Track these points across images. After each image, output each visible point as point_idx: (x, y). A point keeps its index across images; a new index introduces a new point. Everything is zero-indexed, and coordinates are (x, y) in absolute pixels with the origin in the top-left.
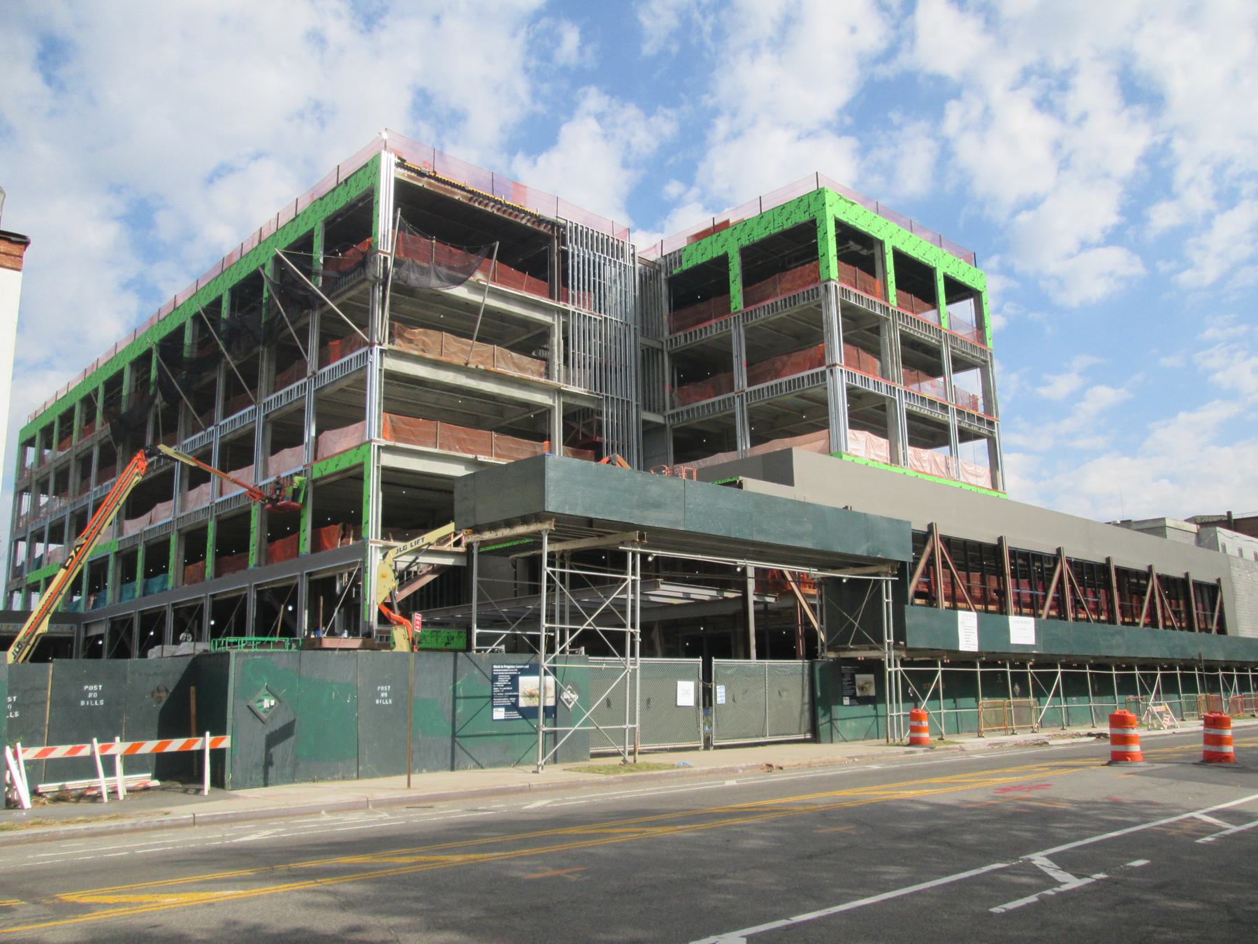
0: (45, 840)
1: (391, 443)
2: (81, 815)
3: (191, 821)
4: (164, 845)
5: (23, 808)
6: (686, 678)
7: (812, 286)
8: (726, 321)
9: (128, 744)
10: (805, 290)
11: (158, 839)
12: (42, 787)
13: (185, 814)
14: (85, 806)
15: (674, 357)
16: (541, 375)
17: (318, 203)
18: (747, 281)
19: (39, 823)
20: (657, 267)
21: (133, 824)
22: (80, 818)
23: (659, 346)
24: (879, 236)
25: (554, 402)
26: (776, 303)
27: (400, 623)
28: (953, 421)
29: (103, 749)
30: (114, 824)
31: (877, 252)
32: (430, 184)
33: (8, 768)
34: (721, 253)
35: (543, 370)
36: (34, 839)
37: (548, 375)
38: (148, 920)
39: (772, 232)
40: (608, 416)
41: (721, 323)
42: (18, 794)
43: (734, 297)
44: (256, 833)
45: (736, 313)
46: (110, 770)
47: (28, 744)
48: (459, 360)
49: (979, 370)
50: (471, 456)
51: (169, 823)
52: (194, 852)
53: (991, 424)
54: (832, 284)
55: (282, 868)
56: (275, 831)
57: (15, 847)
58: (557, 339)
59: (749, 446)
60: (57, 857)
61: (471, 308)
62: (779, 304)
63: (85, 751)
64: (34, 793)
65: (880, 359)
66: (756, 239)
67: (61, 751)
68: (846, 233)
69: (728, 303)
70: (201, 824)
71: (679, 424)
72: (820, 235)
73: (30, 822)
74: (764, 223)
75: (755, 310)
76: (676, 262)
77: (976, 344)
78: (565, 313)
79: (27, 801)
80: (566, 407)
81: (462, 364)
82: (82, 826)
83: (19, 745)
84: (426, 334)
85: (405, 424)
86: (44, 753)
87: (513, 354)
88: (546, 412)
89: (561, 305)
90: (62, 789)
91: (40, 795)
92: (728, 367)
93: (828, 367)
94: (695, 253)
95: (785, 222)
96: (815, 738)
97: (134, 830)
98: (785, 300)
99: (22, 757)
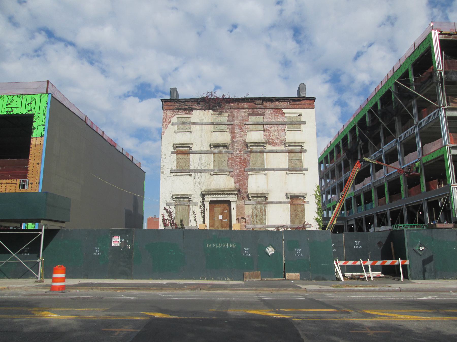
0: (351, 292)
2: (360, 284)
3: (399, 290)
4: (391, 297)
5: (341, 280)
9: (372, 262)
11: (389, 295)
12: (346, 274)
13: (396, 287)
14: (360, 281)
17: (408, 59)
19: (348, 286)
21: (379, 289)
22: (360, 285)
29: (364, 263)
30: (372, 288)
32: (455, 37)
33: (335, 267)
36: (348, 291)
38: (396, 323)
42: (339, 275)
44: (426, 297)
46: (367, 271)
47: (339, 260)
51: (392, 290)
52: (404, 301)
55: (442, 311)
56: (433, 296)
57: (343, 293)
60: (357, 298)
63: (358, 263)
64: (344, 276)
67: (350, 263)
70: (403, 291)
73: (345, 285)
79: (342, 279)
82: (362, 288)
83: (337, 260)
86: (345, 263)
90: (352, 275)
91: (346, 277)
97: (379, 291)
99: (339, 264)
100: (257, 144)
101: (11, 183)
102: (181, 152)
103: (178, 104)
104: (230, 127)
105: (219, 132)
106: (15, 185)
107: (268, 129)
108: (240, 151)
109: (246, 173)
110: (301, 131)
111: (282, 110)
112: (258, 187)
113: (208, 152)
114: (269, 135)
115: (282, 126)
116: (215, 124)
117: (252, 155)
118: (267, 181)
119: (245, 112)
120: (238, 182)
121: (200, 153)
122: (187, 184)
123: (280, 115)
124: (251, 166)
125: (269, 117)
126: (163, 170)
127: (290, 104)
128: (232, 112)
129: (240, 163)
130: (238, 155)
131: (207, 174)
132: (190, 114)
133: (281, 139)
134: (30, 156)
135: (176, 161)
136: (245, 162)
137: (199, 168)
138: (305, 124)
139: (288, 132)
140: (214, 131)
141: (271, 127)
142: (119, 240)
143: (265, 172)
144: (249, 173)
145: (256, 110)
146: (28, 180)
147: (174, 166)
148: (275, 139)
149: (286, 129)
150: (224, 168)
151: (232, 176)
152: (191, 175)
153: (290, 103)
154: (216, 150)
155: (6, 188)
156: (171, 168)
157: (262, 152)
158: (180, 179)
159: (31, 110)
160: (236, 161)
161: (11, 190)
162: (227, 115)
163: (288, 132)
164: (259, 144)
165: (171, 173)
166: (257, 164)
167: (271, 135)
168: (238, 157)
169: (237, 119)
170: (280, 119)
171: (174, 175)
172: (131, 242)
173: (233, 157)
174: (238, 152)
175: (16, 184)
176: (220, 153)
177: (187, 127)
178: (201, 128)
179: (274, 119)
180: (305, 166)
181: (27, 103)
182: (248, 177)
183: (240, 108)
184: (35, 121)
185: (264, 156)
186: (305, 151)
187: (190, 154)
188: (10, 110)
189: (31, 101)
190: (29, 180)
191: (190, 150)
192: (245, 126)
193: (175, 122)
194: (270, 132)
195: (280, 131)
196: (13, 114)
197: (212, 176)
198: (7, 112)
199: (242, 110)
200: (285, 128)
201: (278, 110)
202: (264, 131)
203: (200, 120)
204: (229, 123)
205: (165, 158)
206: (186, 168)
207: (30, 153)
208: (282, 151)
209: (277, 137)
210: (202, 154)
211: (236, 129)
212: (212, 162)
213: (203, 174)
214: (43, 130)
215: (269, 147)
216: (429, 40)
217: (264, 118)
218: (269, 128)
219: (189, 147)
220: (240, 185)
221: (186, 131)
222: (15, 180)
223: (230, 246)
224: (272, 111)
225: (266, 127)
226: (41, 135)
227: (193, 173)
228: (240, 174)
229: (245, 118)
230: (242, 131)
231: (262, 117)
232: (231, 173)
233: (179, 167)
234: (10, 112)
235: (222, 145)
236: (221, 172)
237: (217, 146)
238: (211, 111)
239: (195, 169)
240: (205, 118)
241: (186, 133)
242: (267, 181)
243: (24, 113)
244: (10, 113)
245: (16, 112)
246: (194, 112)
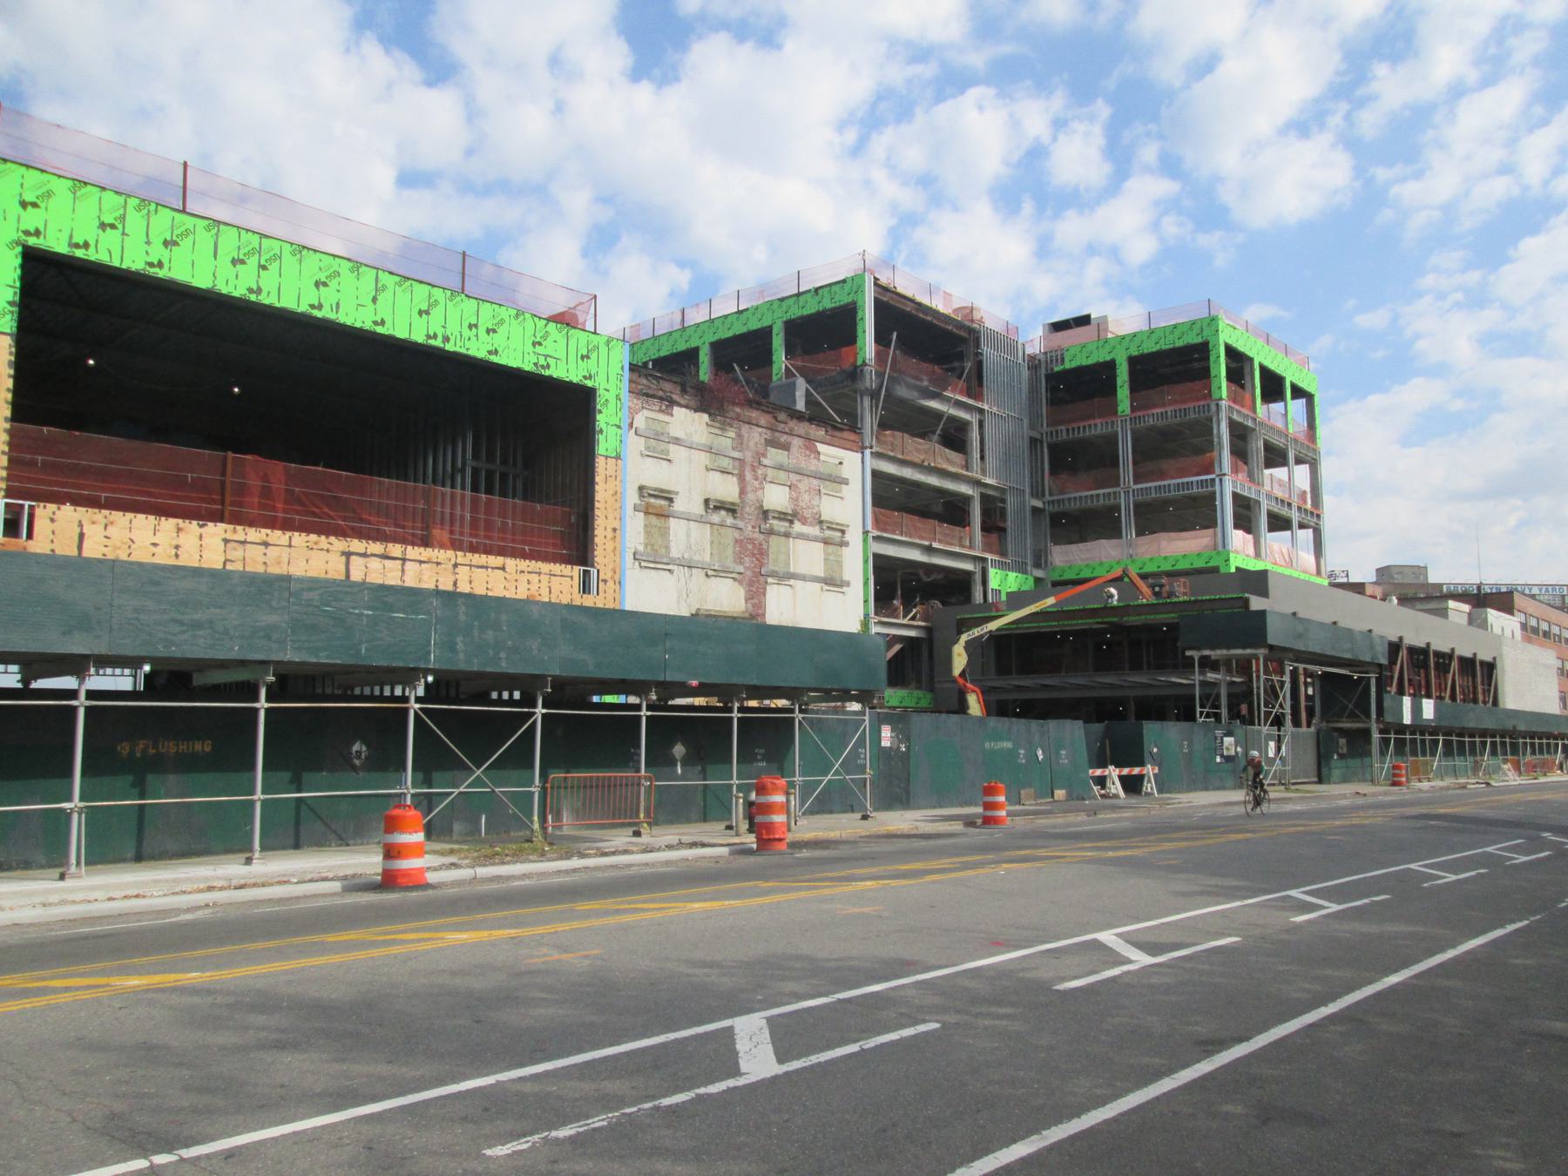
1: (879, 534)
6: (1272, 740)
7: (1202, 403)
8: (1113, 422)
10: (1196, 404)
15: (1050, 447)
16: (962, 468)
17: (776, 305)
18: (1135, 387)
20: (1037, 362)
23: (1038, 437)
24: (1250, 354)
25: (974, 492)
26: (1166, 412)
27: (973, 691)
28: (1295, 516)
31: (1247, 370)
32: (892, 298)
34: (1108, 358)
35: (964, 463)
37: (967, 467)
39: (1164, 347)
40: (1011, 503)
41: (1107, 423)
43: (1121, 401)
45: (1124, 416)
48: (917, 458)
49: (1308, 466)
50: (927, 543)
53: (1318, 516)
54: (1224, 404)
58: (975, 435)
59: (1134, 536)
61: (938, 415)
62: (1169, 413)
65: (1246, 463)
66: (1146, 351)
68: (1231, 352)
69: (1115, 405)
71: (1056, 509)
72: (1212, 358)
74: (1154, 337)
75: (1144, 416)
76: (1057, 360)
77: (1306, 442)
78: (981, 411)
80: (984, 497)
81: (920, 462)
84: (893, 436)
85: (884, 515)
87: (946, 450)
88: (967, 499)
89: (979, 405)
92: (1114, 462)
93: (1218, 476)
94: (1079, 355)
95: (1176, 341)
96: (1320, 781)
98: (1175, 411)
101: (559, 573)
103: (644, 381)
104: (737, 464)
106: (569, 579)
108: (753, 527)
109: (762, 579)
110: (842, 498)
111: (817, 444)
112: (782, 613)
114: (797, 500)
115: (815, 482)
117: (774, 540)
119: (760, 435)
123: (812, 456)
124: (771, 567)
129: (754, 555)
130: (750, 536)
134: (597, 505)
135: (645, 531)
136: (760, 554)
138: (847, 484)
139: (824, 497)
141: (800, 481)
142: (889, 735)
143: (792, 582)
144: (770, 580)
145: (777, 434)
146: (596, 571)
149: (823, 491)
150: (730, 564)
151: (740, 582)
154: (716, 518)
155: (550, 587)
157: (787, 535)
159: (590, 377)
160: (747, 549)
161: (561, 592)
163: (824, 497)
168: (750, 539)
169: (748, 448)
170: (813, 465)
171: (641, 567)
172: (907, 739)
175: (572, 578)
177: (663, 446)
180: (846, 577)
181: (579, 356)
184: (600, 412)
185: (789, 543)
186: (846, 544)
187: (668, 516)
188: (542, 361)
189: (588, 352)
190: (598, 571)
191: (670, 506)
195: (813, 492)
196: (550, 378)
198: (536, 364)
199: (756, 428)
202: (790, 487)
203: (686, 434)
207: (596, 498)
208: (815, 539)
212: (709, 546)
213: (693, 570)
214: (618, 442)
216: (854, 289)
220: (753, 606)
221: (664, 457)
222: (569, 567)
223: (188, 745)
225: (794, 478)
226: (615, 454)
228: (754, 582)
229: (761, 449)
230: (757, 479)
231: (786, 453)
233: (649, 547)
234: (543, 367)
235: (727, 506)
236: (720, 573)
237: (720, 506)
238: (705, 417)
241: (661, 461)
243: (575, 382)
244: (543, 371)
245: (558, 371)
246: (676, 409)
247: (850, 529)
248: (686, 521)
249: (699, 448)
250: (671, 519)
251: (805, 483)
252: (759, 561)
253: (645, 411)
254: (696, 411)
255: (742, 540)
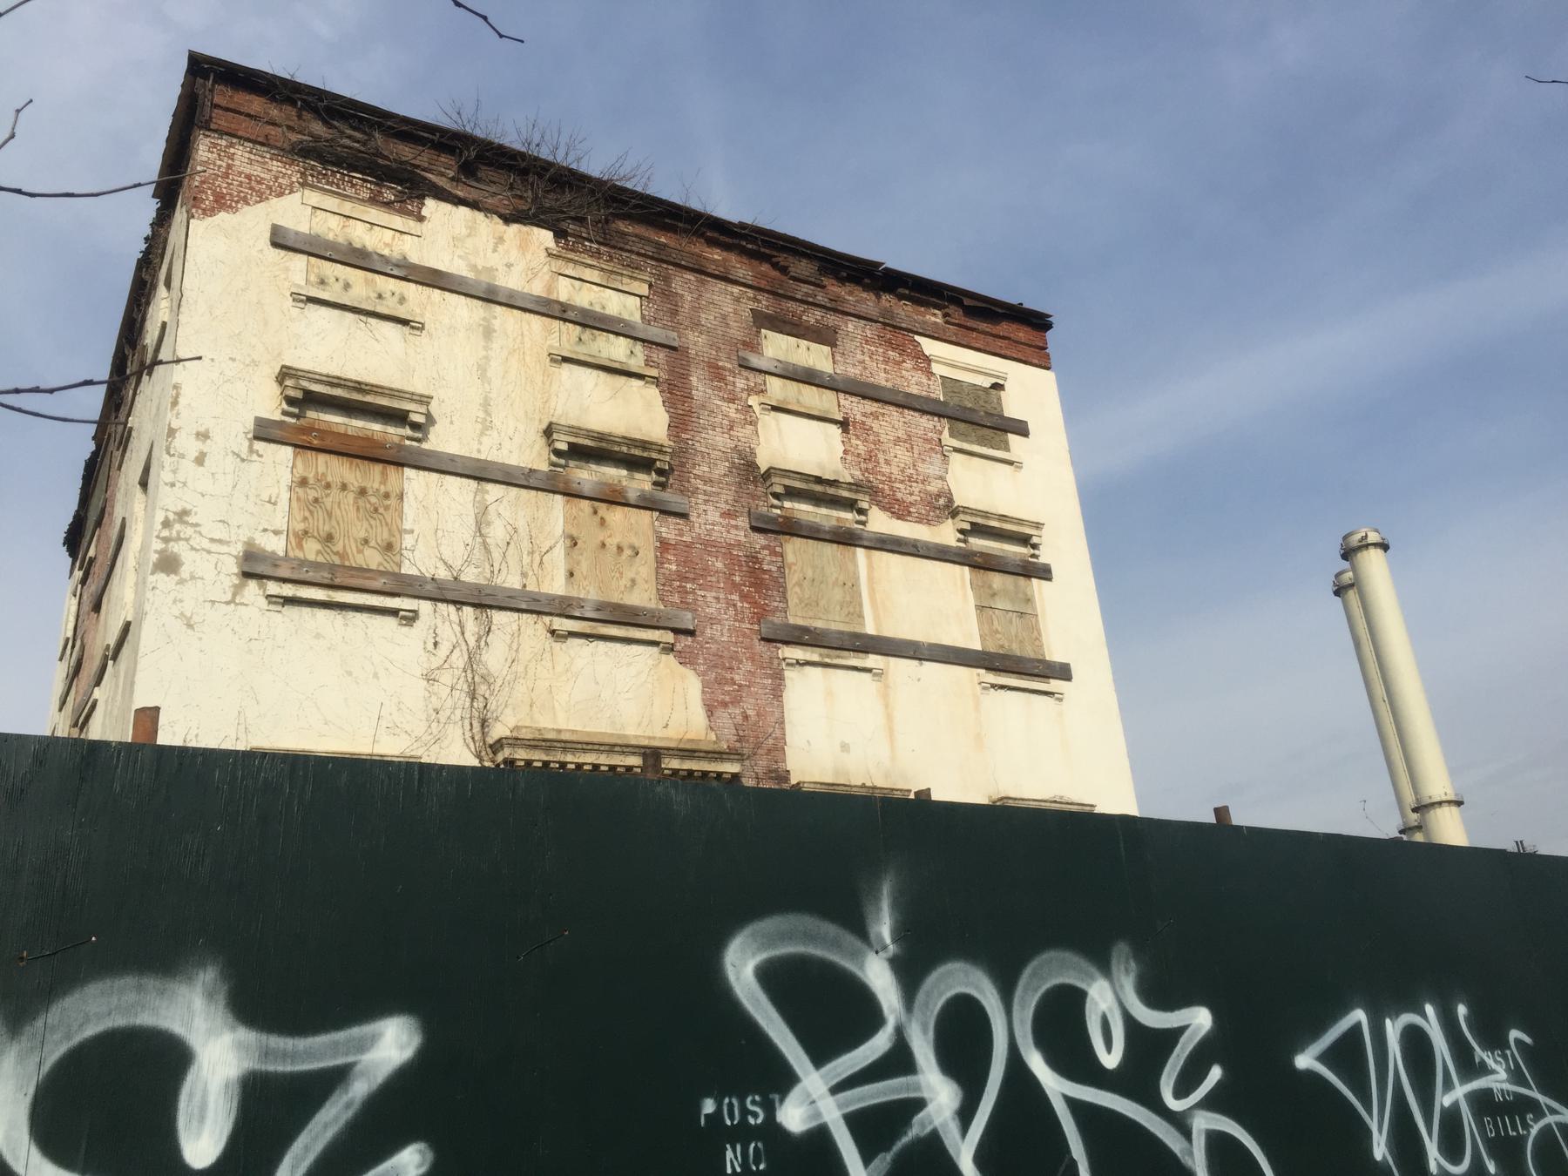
100: (819, 490)
102: (328, 443)
104: (660, 356)
105: (595, 373)
107: (859, 417)
111: (917, 338)
112: (845, 747)
113: (533, 482)
114: (871, 457)
116: (571, 315)
117: (794, 549)
118: (889, 717)
120: (725, 705)
121: (481, 473)
122: (376, 675)
125: (859, 357)
126: (175, 547)
127: (947, 322)
128: (667, 280)
131: (533, 629)
132: (404, 212)
133: (929, 488)
137: (470, 576)
140: (566, 360)
143: (872, 661)
145: (791, 305)
147: (276, 533)
148: (902, 482)
151: (686, 659)
152: (411, 618)
153: (945, 315)
154: (587, 475)
156: (250, 544)
157: (846, 539)
158: (318, 636)
162: (644, 289)
164: (831, 491)
165: (247, 575)
166: (822, 603)
167: (881, 457)
169: (696, 325)
170: (913, 383)
173: (687, 538)
174: (714, 516)
176: (613, 498)
178: (484, 319)
179: (883, 375)
182: (782, 678)
183: (712, 268)
186: (1045, 573)
192: (745, 373)
193: (297, 233)
194: (872, 438)
195: (919, 446)
197: (557, 646)
199: (721, 285)
200: (941, 433)
201: (898, 337)
204: (655, 333)
205: (200, 460)
206: (372, 559)
208: (940, 554)
209: (909, 472)
210: (490, 487)
211: (694, 379)
212: (559, 552)
213: (499, 617)
215: (880, 522)
217: (838, 357)
218: (864, 415)
219: (399, 418)
224: (870, 331)
225: (856, 408)
227: (425, 607)
231: (827, 349)
232: (682, 637)
238: (544, 237)
239: (443, 574)
240: (509, 266)
242: (889, 717)
246: (431, 206)
247: (1045, 532)
248: (473, 484)
249: (529, 306)
250: (408, 472)
251: (891, 423)
252: (755, 604)
253: (307, 192)
254: (507, 220)
255: (689, 546)
